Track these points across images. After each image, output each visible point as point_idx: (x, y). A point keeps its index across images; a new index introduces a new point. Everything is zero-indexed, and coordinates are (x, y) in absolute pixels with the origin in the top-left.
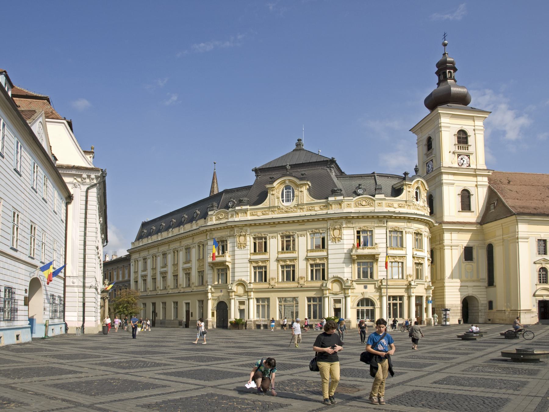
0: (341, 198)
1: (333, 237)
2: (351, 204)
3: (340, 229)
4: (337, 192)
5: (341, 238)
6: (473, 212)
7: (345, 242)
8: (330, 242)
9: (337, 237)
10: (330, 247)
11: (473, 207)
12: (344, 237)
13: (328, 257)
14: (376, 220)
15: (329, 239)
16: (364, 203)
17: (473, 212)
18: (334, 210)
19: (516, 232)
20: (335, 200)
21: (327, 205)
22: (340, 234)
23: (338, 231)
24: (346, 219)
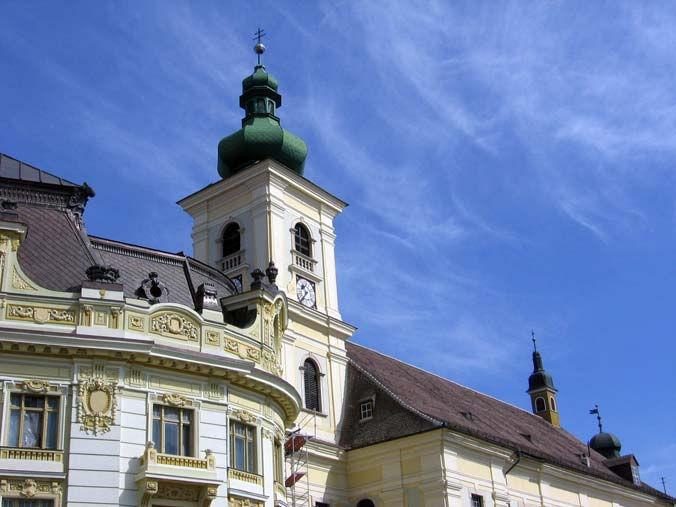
0: (117, 296)
1: (89, 413)
2: (142, 320)
3: (109, 392)
4: (107, 278)
5: (111, 421)
6: (325, 416)
7: (124, 435)
8: (75, 429)
9: (101, 414)
10: (74, 446)
11: (325, 409)
12: (121, 419)
13: (67, 479)
14: (203, 381)
15: (73, 419)
16: (174, 326)
17: (325, 416)
18: (96, 328)
19: (439, 470)
20: (101, 299)
21: (78, 309)
22: (110, 405)
23: (104, 395)
24: (129, 362)
